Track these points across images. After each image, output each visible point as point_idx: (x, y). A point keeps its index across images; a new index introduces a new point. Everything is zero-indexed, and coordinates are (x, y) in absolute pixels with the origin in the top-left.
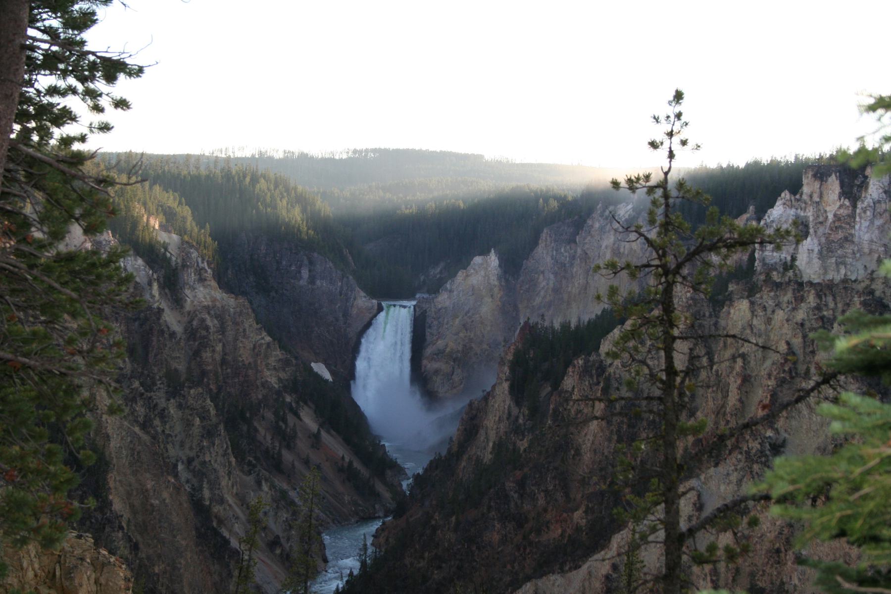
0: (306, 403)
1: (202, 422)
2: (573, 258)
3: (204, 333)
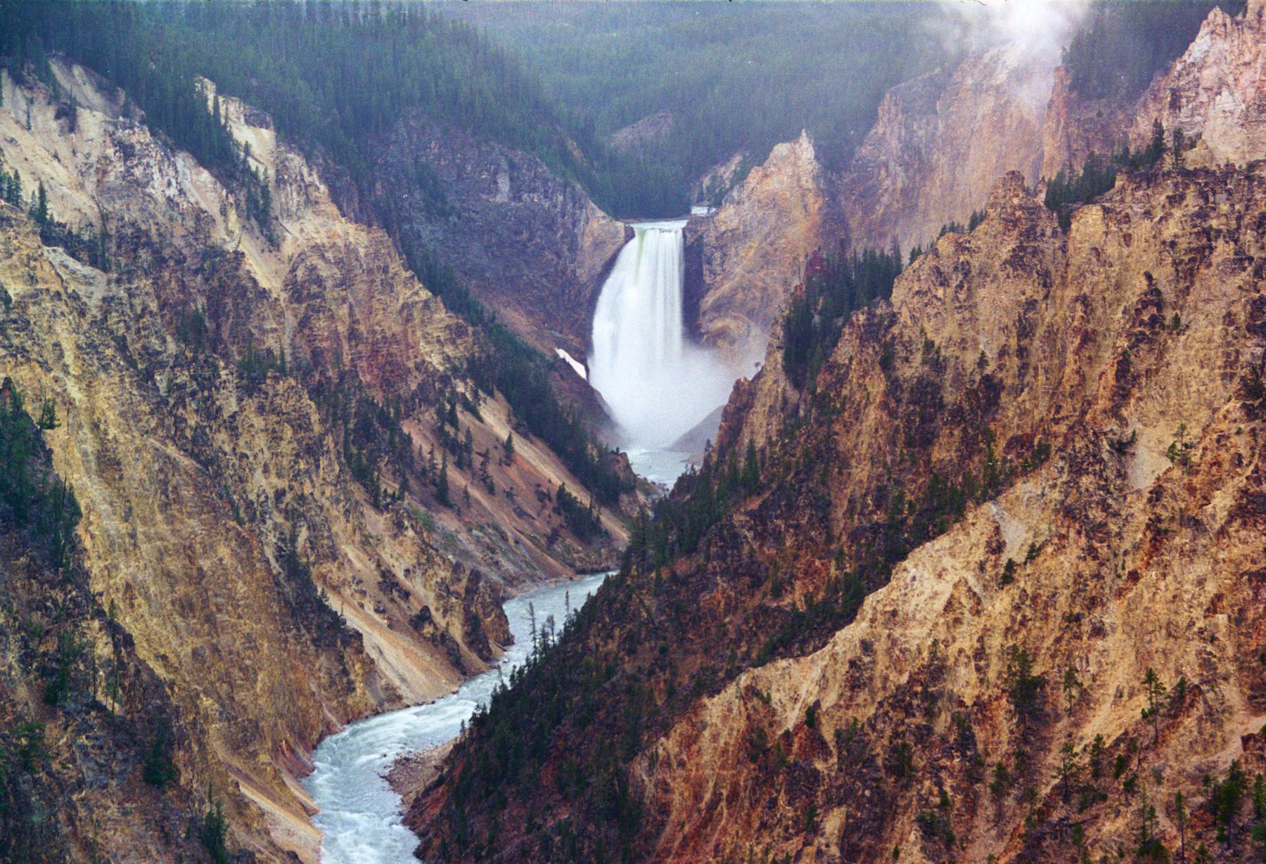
0: (491, 394)
1: (295, 432)
3: (314, 289)
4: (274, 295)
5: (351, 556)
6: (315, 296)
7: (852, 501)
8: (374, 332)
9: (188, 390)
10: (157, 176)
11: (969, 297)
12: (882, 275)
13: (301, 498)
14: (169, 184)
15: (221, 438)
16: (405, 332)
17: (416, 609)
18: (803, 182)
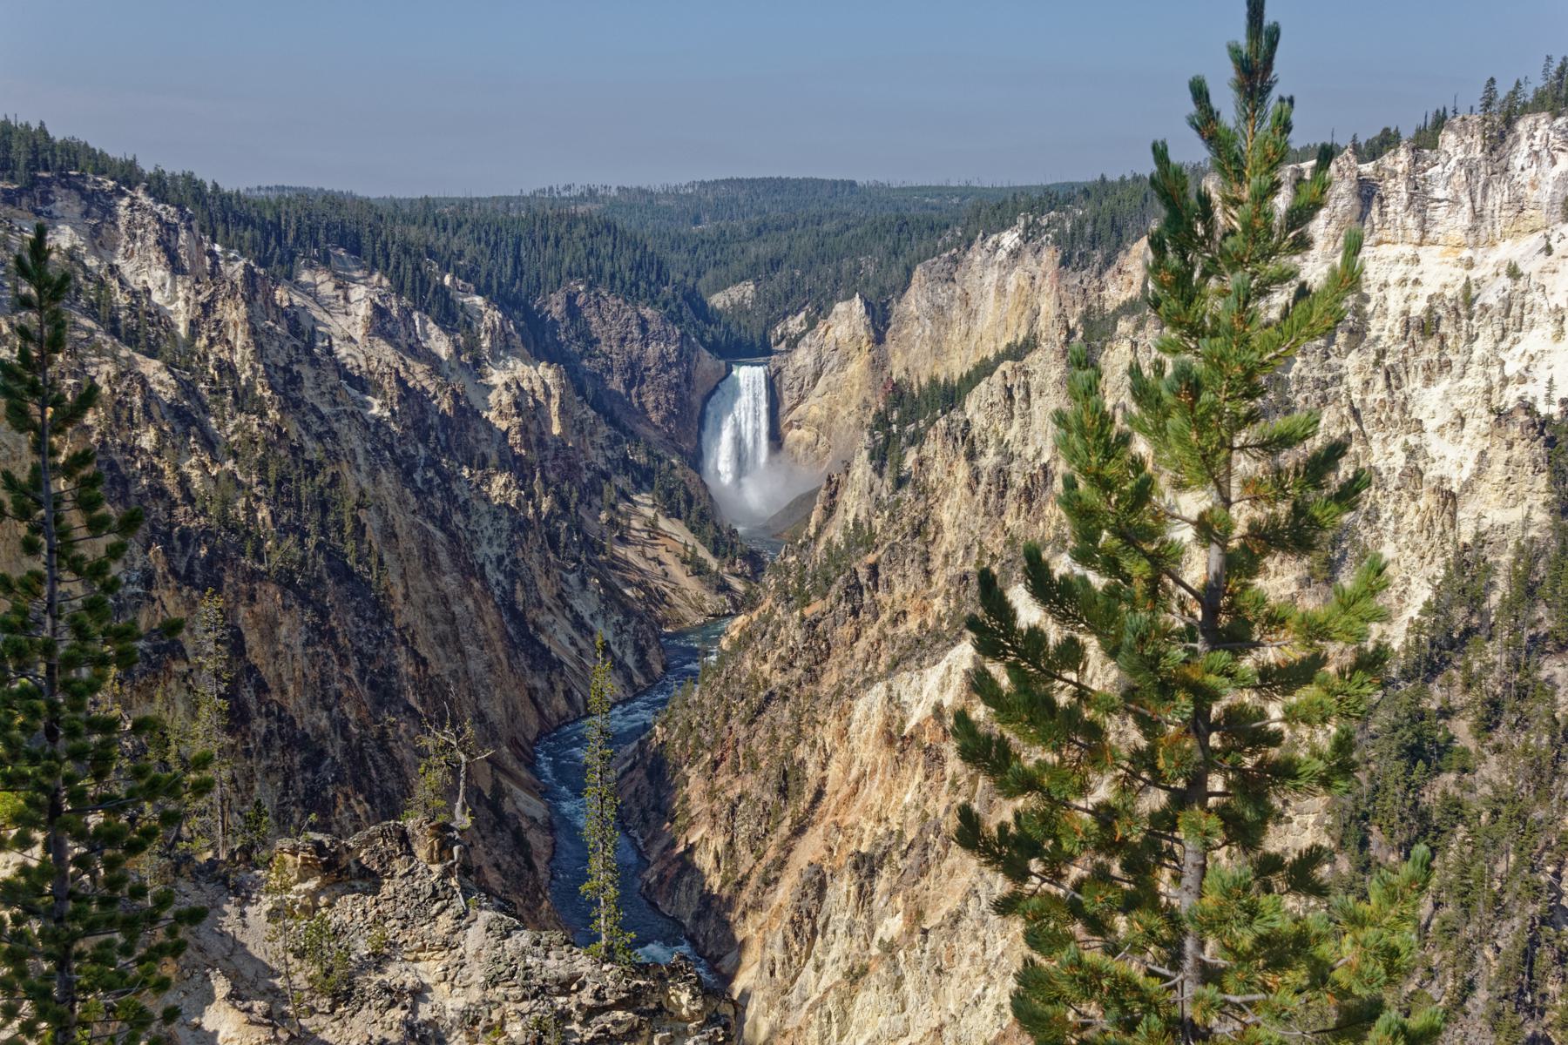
2: (952, 299)
7: (946, 556)
12: (950, 396)
13: (515, 562)
15: (458, 518)
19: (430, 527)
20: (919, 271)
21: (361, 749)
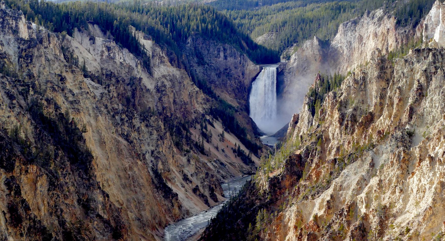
0: (218, 120)
3: (163, 89)
4: (151, 91)
5: (174, 170)
6: (163, 91)
8: (181, 101)
9: (125, 120)
10: (117, 56)
11: (365, 87)
13: (159, 152)
14: (121, 58)
15: (134, 135)
16: (191, 101)
17: (194, 187)
18: (315, 53)
19: (120, 139)
20: (341, 27)
21: (70, 233)
